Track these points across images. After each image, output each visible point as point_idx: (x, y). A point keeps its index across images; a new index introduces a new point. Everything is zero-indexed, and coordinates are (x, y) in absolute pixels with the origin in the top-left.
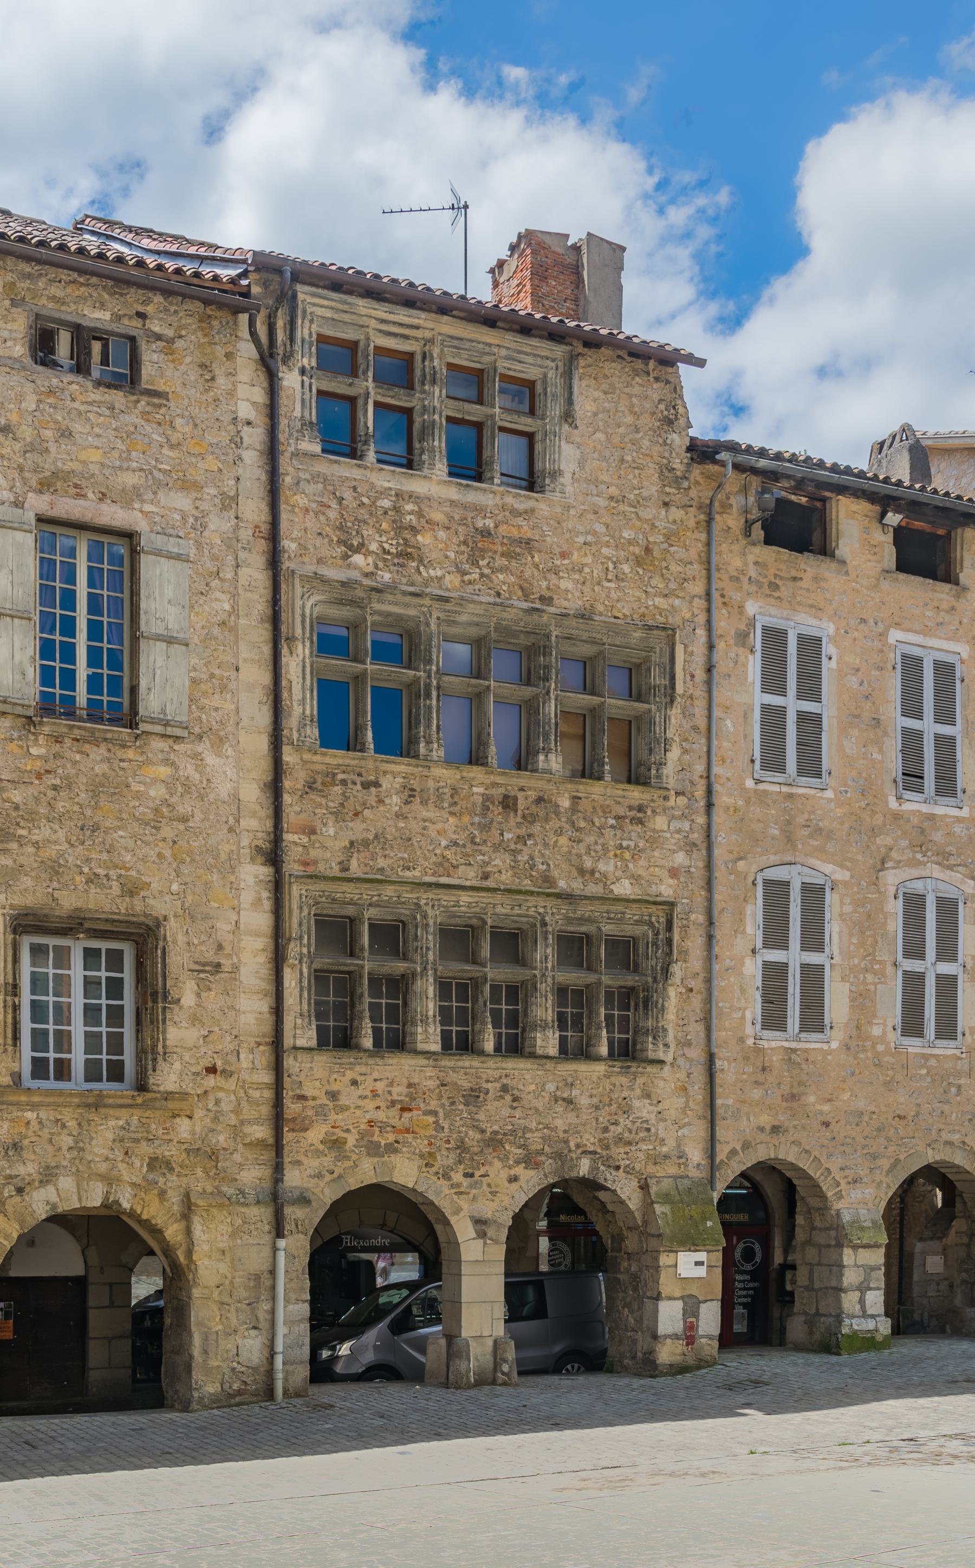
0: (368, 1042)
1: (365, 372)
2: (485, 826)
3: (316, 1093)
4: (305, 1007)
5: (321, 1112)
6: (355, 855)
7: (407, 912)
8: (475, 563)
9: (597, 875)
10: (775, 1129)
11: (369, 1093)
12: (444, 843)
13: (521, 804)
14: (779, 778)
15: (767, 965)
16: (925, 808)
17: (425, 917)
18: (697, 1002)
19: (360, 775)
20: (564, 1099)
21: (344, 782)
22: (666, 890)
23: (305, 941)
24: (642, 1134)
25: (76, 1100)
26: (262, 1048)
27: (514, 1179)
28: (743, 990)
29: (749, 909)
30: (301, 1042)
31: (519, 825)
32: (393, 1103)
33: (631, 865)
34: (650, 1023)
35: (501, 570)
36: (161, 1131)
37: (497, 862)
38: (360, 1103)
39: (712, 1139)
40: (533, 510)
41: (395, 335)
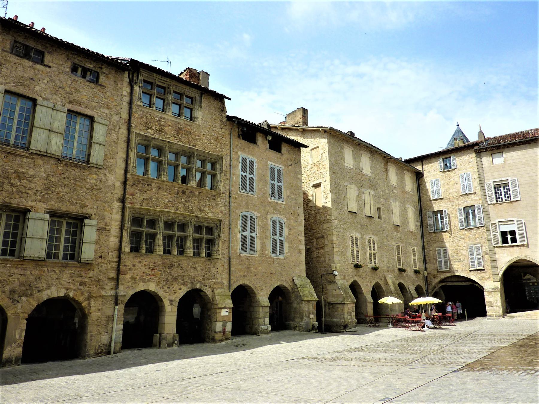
0: (144, 251)
1: (154, 89)
2: (177, 197)
3: (129, 264)
4: (128, 241)
5: (130, 269)
6: (144, 202)
7: (156, 217)
8: (178, 135)
9: (204, 211)
11: (143, 265)
12: (167, 201)
13: (186, 193)
15: (242, 236)
17: (161, 219)
18: (226, 243)
19: (147, 182)
20: (194, 268)
21: (143, 184)
22: (220, 216)
23: (129, 223)
25: (60, 265)
26: (115, 251)
28: (237, 242)
31: (186, 198)
33: (212, 209)
34: (215, 249)
35: (184, 138)
36: (84, 274)
37: (180, 206)
38: (141, 267)
40: (192, 125)
41: (162, 82)
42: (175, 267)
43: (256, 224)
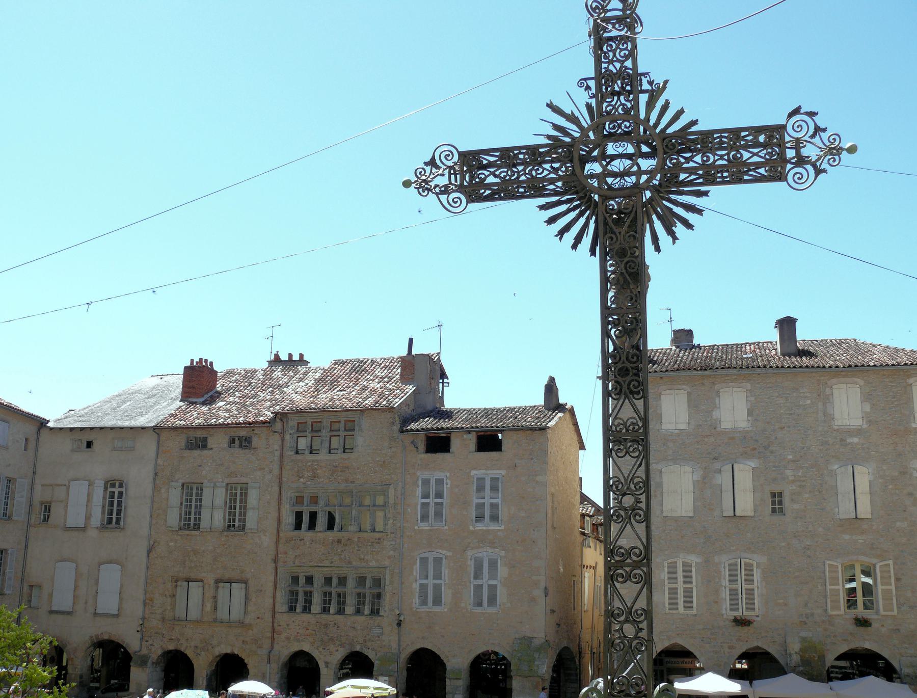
10: (423, 638)
11: (297, 624)
14: (427, 525)
15: (421, 585)
16: (485, 528)
22: (387, 563)
24: (377, 638)
27: (337, 651)
29: (415, 567)
30: (280, 611)
32: (304, 627)
35: (341, 476)
39: (399, 640)
42: (331, 625)
43: (443, 568)
